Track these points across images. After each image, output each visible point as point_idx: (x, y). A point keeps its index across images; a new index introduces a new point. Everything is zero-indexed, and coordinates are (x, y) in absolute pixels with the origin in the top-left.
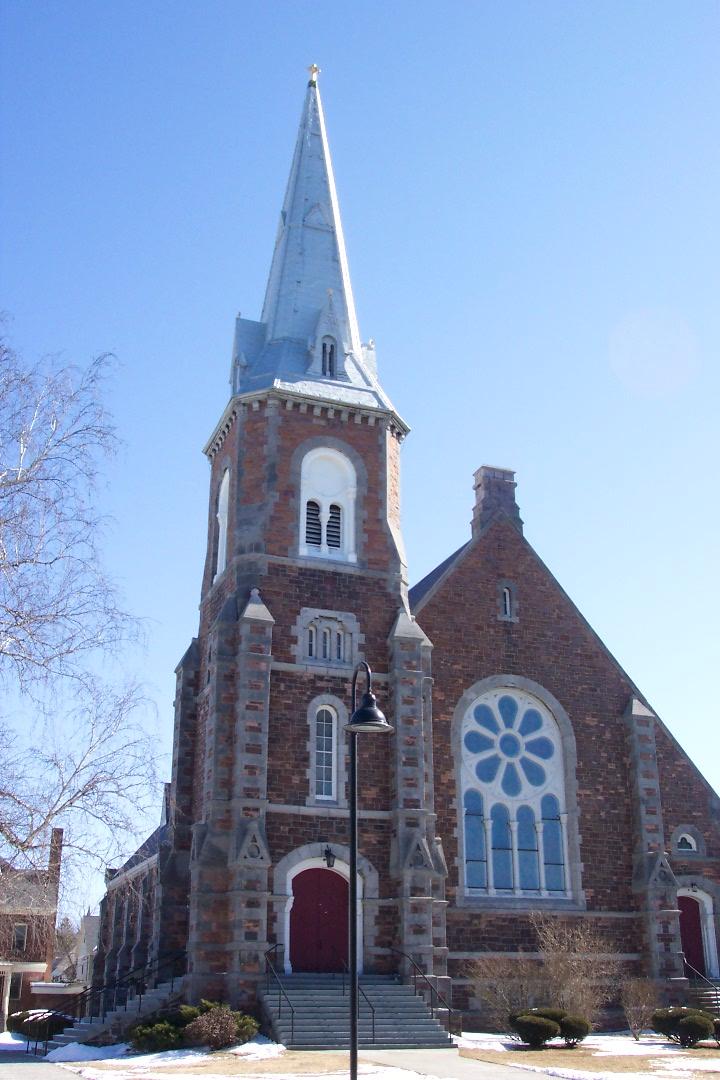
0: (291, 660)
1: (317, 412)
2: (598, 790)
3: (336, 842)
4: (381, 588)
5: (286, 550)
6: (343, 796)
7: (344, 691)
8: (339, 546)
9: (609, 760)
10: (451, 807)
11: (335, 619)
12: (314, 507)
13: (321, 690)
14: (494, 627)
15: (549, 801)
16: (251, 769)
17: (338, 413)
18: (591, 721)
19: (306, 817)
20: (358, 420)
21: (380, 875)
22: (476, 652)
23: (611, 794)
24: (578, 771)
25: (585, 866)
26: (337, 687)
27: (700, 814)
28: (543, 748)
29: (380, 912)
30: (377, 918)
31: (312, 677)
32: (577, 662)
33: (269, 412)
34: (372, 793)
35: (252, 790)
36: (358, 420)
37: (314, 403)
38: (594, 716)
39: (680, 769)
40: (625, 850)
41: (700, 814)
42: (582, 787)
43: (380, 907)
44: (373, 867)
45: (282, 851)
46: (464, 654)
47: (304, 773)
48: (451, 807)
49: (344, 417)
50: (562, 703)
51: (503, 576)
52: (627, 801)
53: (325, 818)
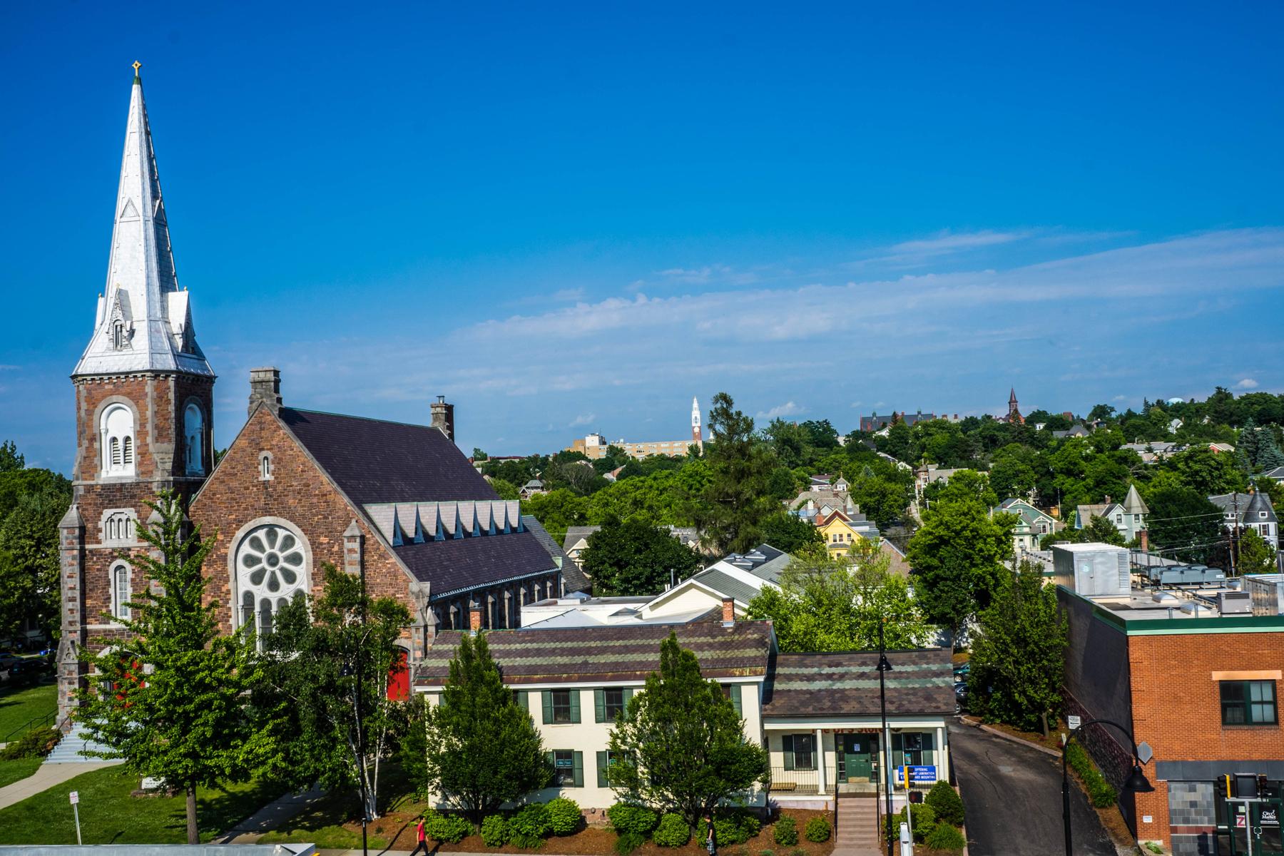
0: (99, 542)
4: (149, 489)
5: (93, 475)
7: (129, 556)
10: (228, 606)
12: (114, 439)
13: (116, 557)
14: (256, 486)
16: (72, 611)
18: (324, 540)
19: (110, 631)
22: (244, 505)
24: (313, 574)
26: (124, 553)
27: (402, 596)
28: (296, 559)
31: (110, 550)
32: (315, 500)
35: (73, 622)
38: (325, 536)
39: (389, 566)
41: (402, 596)
42: (315, 586)
45: (98, 650)
46: (236, 508)
47: (108, 606)
48: (228, 606)
50: (303, 530)
51: (262, 449)
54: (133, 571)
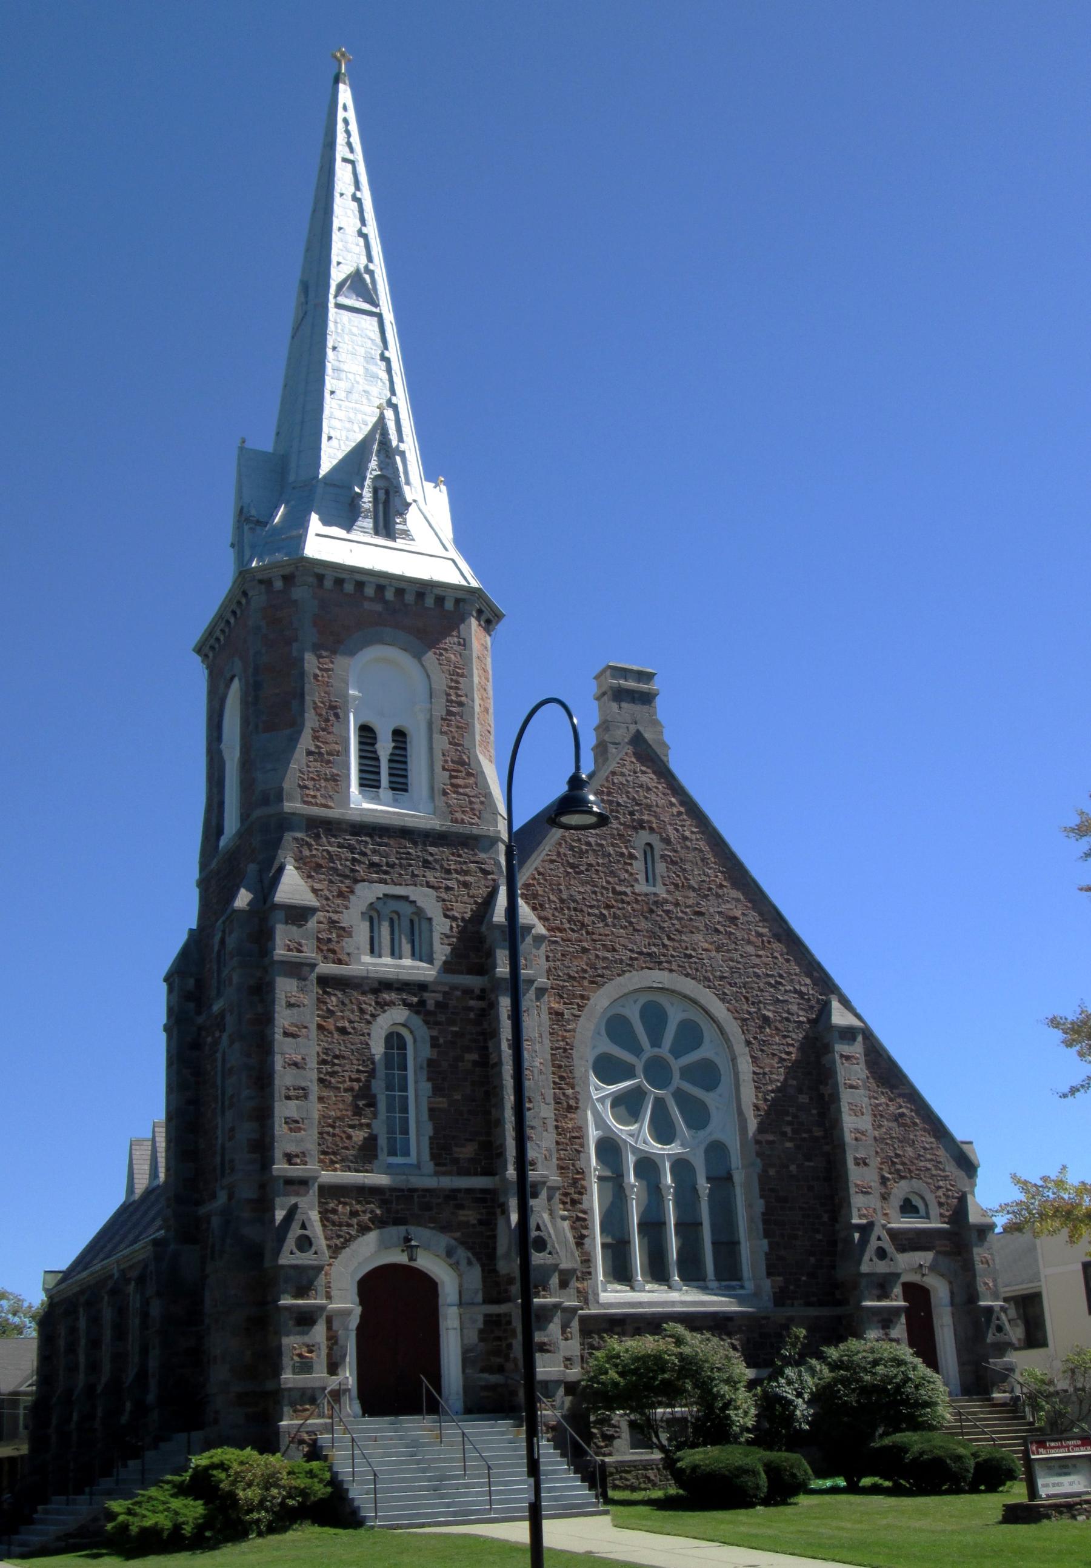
1: (370, 591)
2: (784, 1134)
3: (419, 1224)
6: (426, 1156)
8: (406, 790)
9: (800, 1091)
11: (405, 898)
15: (716, 1151)
17: (400, 592)
20: (429, 602)
21: (483, 1271)
23: (804, 1139)
25: (770, 1244)
29: (486, 1322)
30: (481, 1332)
31: (376, 985)
33: (299, 593)
34: (466, 1151)
36: (429, 602)
37: (364, 578)
40: (825, 1218)
43: (486, 1316)
44: (474, 1260)
49: (409, 598)
51: (640, 825)
52: (827, 1148)
53: (402, 1190)
54: (434, 1043)
